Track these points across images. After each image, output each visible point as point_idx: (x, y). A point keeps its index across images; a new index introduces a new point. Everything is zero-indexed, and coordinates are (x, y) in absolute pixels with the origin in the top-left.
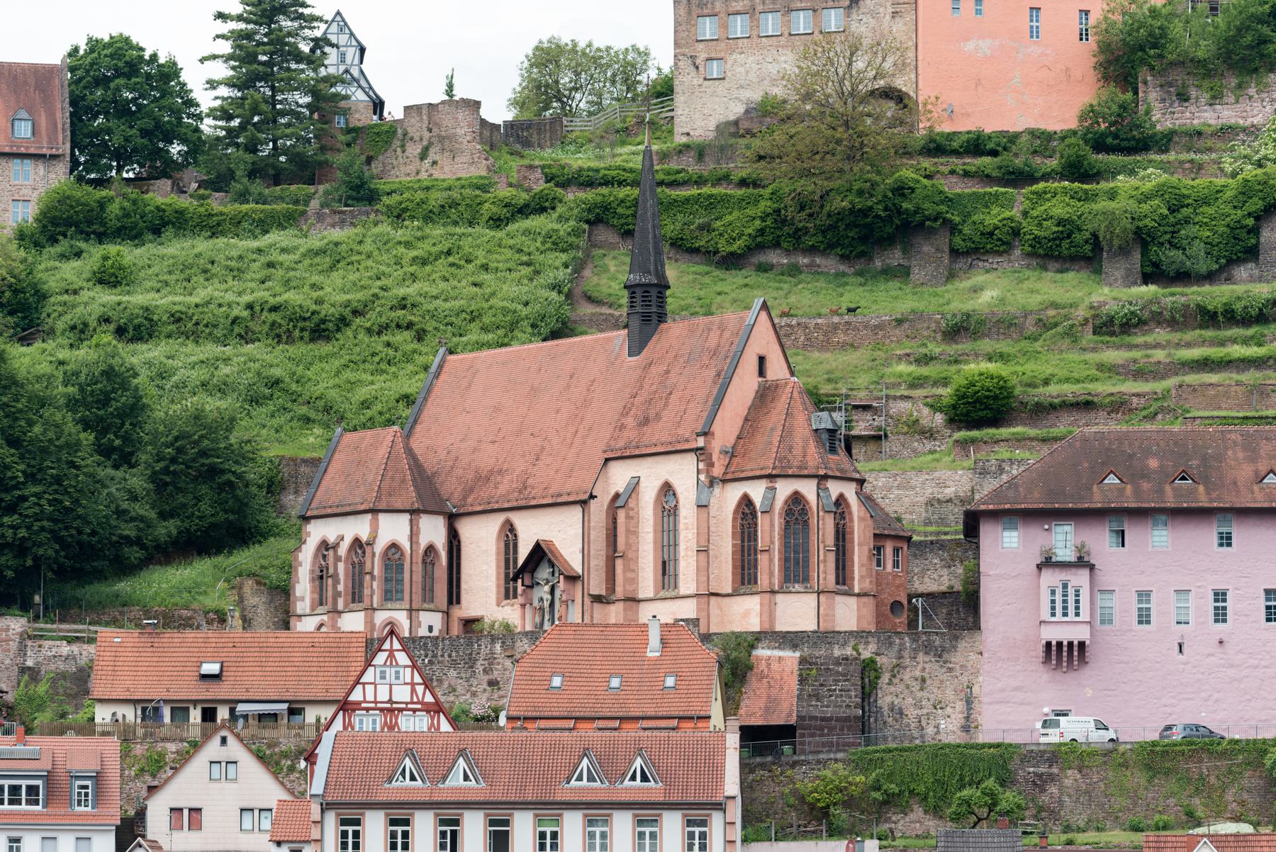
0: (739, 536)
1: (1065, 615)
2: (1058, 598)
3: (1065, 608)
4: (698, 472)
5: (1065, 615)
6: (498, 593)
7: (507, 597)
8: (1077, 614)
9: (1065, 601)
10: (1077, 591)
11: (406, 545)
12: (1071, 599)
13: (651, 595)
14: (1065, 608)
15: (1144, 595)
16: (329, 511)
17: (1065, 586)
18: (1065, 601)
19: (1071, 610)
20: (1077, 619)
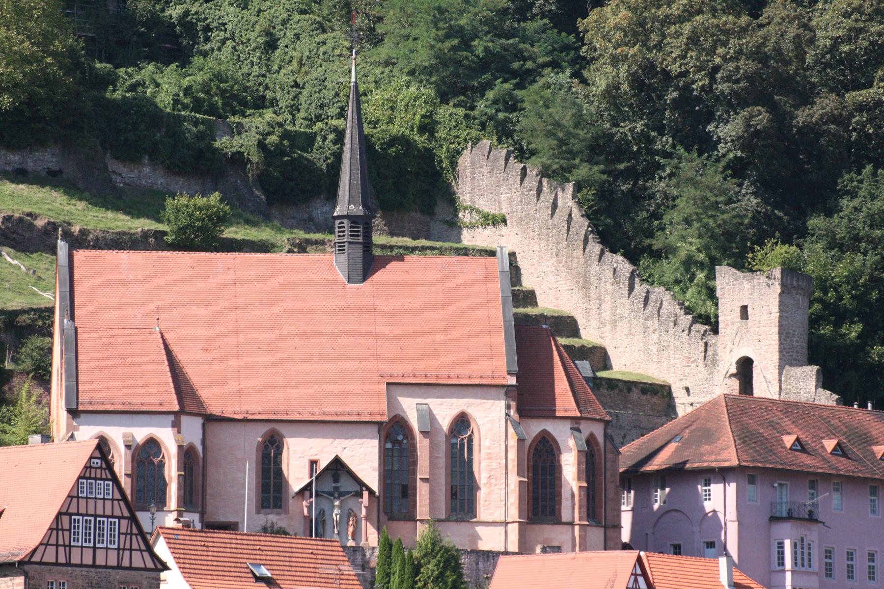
0: (531, 469)
1: (803, 565)
2: (799, 550)
3: (803, 559)
4: (508, 407)
5: (803, 565)
6: (257, 502)
7: (263, 507)
8: (810, 566)
9: (803, 553)
10: (809, 545)
11: (200, 448)
12: (806, 551)
13: (443, 517)
14: (803, 559)
15: (829, 553)
16: (112, 408)
17: (802, 540)
18: (803, 553)
19: (806, 562)
20: (810, 570)
